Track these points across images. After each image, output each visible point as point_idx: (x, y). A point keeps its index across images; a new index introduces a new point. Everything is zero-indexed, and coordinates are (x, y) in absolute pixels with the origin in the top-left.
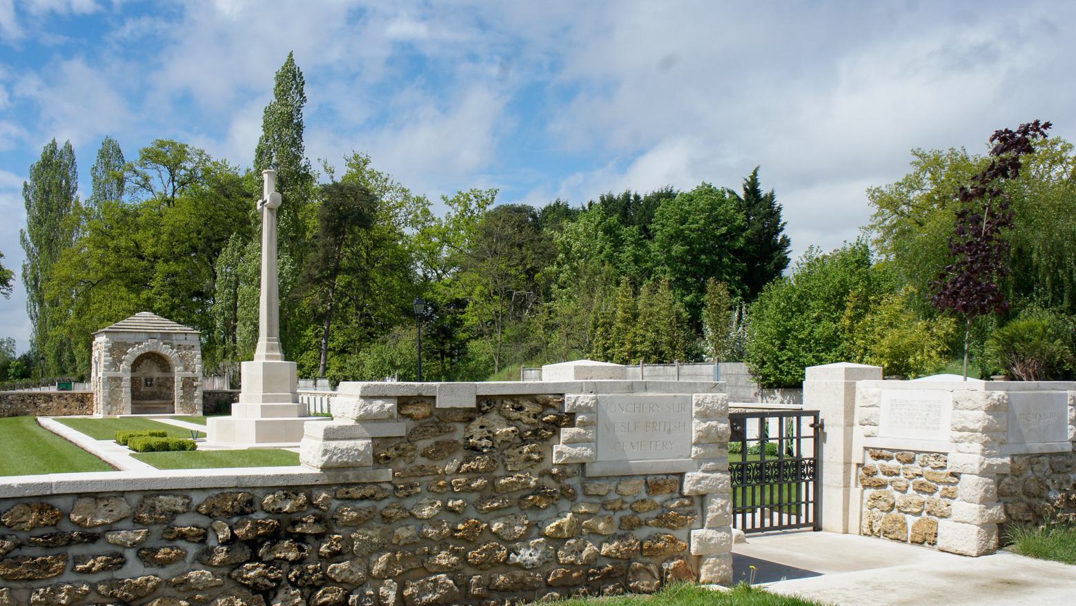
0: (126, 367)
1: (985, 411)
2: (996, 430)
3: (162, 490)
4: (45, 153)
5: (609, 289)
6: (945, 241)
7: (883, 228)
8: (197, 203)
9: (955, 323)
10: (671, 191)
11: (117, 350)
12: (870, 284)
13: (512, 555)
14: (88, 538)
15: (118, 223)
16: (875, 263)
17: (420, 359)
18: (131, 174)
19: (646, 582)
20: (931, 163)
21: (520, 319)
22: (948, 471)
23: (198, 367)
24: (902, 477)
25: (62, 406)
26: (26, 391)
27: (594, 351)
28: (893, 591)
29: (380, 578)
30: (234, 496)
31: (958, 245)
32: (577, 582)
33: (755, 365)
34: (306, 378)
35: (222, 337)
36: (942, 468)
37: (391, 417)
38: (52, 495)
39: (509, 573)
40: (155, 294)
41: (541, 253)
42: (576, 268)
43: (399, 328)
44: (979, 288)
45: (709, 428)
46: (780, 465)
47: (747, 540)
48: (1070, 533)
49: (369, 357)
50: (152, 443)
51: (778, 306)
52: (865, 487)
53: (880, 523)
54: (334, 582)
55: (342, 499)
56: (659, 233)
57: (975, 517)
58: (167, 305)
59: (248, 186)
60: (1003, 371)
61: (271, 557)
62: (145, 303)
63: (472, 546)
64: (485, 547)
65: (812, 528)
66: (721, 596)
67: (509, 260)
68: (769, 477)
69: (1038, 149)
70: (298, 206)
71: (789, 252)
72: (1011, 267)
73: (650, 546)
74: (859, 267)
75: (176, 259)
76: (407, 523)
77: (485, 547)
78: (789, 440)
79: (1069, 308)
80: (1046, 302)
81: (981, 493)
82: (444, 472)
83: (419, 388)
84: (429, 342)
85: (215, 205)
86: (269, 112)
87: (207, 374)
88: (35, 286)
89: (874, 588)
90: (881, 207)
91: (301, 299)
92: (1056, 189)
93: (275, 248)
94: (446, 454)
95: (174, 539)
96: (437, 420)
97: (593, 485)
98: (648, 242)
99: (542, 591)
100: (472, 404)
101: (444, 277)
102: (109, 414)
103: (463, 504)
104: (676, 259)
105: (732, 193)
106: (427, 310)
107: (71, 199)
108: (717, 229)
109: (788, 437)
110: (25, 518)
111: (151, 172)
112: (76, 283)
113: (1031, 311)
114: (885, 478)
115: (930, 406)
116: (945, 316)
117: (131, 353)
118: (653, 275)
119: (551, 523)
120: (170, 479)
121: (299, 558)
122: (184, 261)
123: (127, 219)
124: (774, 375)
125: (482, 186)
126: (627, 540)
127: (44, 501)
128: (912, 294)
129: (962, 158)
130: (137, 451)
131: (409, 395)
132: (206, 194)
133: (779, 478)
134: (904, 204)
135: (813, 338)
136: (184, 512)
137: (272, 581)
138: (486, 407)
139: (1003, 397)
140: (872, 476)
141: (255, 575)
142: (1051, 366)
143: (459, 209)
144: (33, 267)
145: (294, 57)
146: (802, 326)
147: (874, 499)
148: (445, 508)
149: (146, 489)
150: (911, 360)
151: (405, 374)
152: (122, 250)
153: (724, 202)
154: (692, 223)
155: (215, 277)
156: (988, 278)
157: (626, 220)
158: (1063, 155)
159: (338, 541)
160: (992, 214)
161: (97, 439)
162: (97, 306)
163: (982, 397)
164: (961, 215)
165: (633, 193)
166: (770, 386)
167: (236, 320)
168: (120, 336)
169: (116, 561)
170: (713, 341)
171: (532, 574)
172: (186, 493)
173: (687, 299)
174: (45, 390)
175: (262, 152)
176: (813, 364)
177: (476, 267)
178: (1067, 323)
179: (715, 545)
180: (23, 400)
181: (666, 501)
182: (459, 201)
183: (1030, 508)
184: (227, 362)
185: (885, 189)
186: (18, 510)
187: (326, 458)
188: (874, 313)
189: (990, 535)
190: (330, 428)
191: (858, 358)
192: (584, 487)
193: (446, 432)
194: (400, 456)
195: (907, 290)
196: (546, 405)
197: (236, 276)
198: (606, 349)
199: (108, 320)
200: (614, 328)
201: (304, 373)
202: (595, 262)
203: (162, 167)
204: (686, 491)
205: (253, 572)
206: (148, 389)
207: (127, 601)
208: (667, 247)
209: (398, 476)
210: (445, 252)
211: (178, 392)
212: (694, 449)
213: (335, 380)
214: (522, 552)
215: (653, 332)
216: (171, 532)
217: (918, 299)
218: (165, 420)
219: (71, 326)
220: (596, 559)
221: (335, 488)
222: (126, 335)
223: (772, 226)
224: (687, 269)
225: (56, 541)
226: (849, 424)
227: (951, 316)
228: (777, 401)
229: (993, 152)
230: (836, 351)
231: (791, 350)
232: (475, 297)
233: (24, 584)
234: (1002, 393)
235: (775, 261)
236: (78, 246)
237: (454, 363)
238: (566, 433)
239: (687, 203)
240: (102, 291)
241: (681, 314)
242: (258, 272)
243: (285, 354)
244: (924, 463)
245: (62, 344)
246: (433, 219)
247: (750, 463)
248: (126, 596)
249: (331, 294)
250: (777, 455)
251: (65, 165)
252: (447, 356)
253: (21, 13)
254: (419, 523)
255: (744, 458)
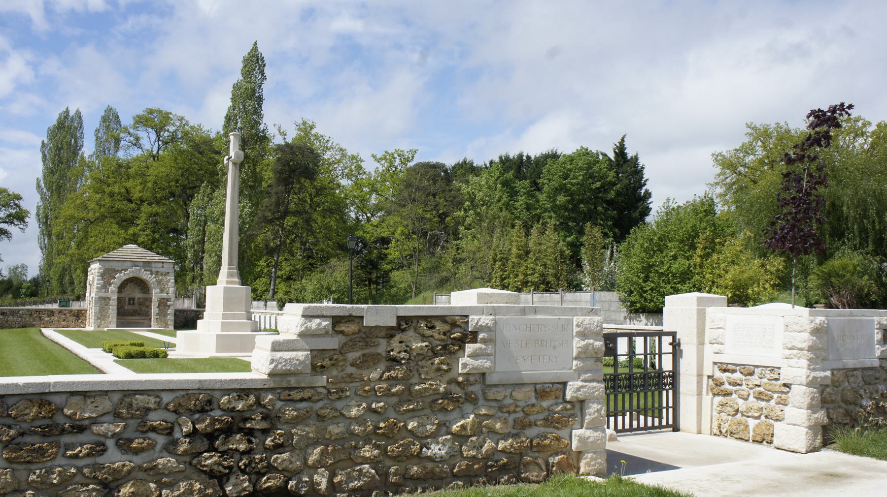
0: (114, 289)
1: (810, 333)
2: (819, 349)
3: (138, 390)
4: (60, 118)
5: (506, 230)
6: (774, 195)
7: (725, 184)
8: (176, 158)
9: (784, 261)
10: (556, 153)
11: (107, 275)
12: (715, 229)
13: (424, 449)
14: (77, 428)
15: (113, 173)
16: (719, 213)
17: (351, 286)
18: (126, 135)
19: (535, 474)
20: (761, 134)
21: (433, 254)
22: (781, 382)
23: (172, 290)
24: (744, 387)
25: (62, 320)
26: (34, 307)
27: (493, 281)
28: (738, 482)
29: (315, 468)
30: (197, 396)
31: (785, 199)
32: (478, 473)
33: (624, 293)
34: (259, 300)
35: (192, 265)
36: (776, 379)
37: (327, 333)
38: (50, 393)
39: (422, 465)
40: (140, 230)
41: (451, 201)
42: (479, 213)
43: (335, 260)
44: (802, 234)
45: (587, 345)
46: (645, 376)
47: (618, 438)
48: (880, 433)
49: (310, 284)
50: (132, 351)
51: (642, 246)
52: (714, 395)
53: (727, 425)
54: (276, 470)
55: (284, 400)
56: (546, 186)
57: (804, 420)
58: (149, 239)
59: (217, 145)
60: (823, 301)
61: (225, 448)
62: (132, 238)
63: (391, 441)
64: (402, 442)
65: (671, 429)
66: (597, 485)
67: (425, 207)
68: (636, 387)
69: (844, 125)
70: (257, 162)
71: (650, 203)
72: (827, 217)
73: (538, 443)
74: (706, 215)
75: (158, 202)
76: (338, 421)
77: (402, 442)
78: (653, 356)
79: (873, 250)
80: (855, 246)
81: (807, 400)
82: (369, 379)
83: (350, 309)
84: (359, 272)
85: (190, 160)
86: (236, 87)
87: (178, 296)
88: (46, 222)
89: (723, 480)
90: (724, 168)
91: (257, 235)
92: (860, 156)
93: (237, 194)
94: (371, 364)
95: (146, 432)
96: (364, 336)
97: (491, 392)
98: (537, 193)
99: (448, 480)
100: (393, 323)
101: (372, 219)
102: (98, 327)
103: (384, 406)
104: (560, 207)
105: (605, 155)
106: (358, 246)
107: (78, 154)
108: (593, 183)
109: (651, 353)
110: (27, 411)
111: (142, 134)
112: (78, 220)
113: (844, 252)
114: (731, 387)
115: (766, 329)
116: (776, 256)
117: (119, 278)
118: (541, 220)
119: (457, 422)
120: (145, 381)
121: (248, 449)
122: (164, 204)
123: (121, 170)
124: (640, 302)
125: (405, 147)
126: (519, 437)
127: (43, 397)
128: (750, 237)
129: (785, 131)
130: (120, 358)
131: (342, 315)
132: (184, 151)
133: (645, 387)
134: (741, 166)
135: (671, 273)
136: (155, 409)
137: (225, 468)
138: (405, 326)
139: (824, 322)
140: (720, 386)
141: (211, 464)
142: (861, 297)
143: (386, 165)
144: (45, 208)
145: (258, 46)
146: (662, 262)
147: (722, 405)
148: (369, 409)
149: (126, 389)
150: (750, 291)
151: (339, 298)
152: (115, 195)
153: (598, 162)
154: (573, 179)
155: (188, 218)
156: (809, 225)
157: (519, 175)
158: (864, 130)
159: (281, 435)
160: (810, 175)
161: (88, 347)
162: (93, 239)
163: (807, 322)
164: (787, 175)
165: (525, 154)
166: (637, 311)
167: (203, 252)
168: (111, 264)
169: (99, 449)
170: (590, 273)
171: (440, 465)
172: (158, 393)
173: (569, 239)
174: (49, 306)
175: (230, 119)
176: (671, 294)
177: (398, 211)
178: (872, 263)
179: (592, 442)
180: (31, 315)
181: (552, 405)
182: (385, 158)
183: (847, 413)
184: (195, 286)
185: (725, 154)
186: (22, 405)
187: (272, 366)
188: (719, 252)
189: (816, 435)
190: (277, 342)
191: (707, 289)
192: (484, 394)
193: (371, 346)
194: (333, 365)
195: (745, 234)
196: (454, 325)
197: (205, 216)
198: (503, 279)
199: (101, 251)
200: (510, 263)
201: (257, 296)
202: (494, 209)
203: (150, 130)
204: (568, 397)
205: (210, 460)
206: (131, 307)
207: (106, 482)
208: (552, 197)
209: (332, 382)
210: (374, 199)
211: (154, 310)
212: (575, 362)
213: (282, 301)
214: (432, 447)
215: (541, 265)
216: (145, 426)
217: (755, 241)
218: (143, 332)
219: (72, 255)
220: (494, 454)
221: (279, 391)
222: (115, 263)
223: (637, 182)
224: (569, 215)
225: (51, 431)
226: (701, 343)
227: (781, 255)
228: (642, 324)
229: (809, 127)
230: (689, 283)
231: (653, 282)
232: (397, 236)
233: (24, 466)
234: (823, 318)
235: (640, 210)
236: (81, 192)
237: (379, 289)
238: (470, 348)
239: (569, 163)
240: (98, 228)
241: (564, 251)
242: (223, 214)
243: (242, 280)
244: (762, 376)
245: (64, 269)
246: (365, 173)
247: (621, 374)
248: (106, 478)
249: (280, 232)
250: (642, 368)
251: (75, 127)
252: (374, 283)
253: (49, 11)
254: (348, 421)
255: (616, 370)
